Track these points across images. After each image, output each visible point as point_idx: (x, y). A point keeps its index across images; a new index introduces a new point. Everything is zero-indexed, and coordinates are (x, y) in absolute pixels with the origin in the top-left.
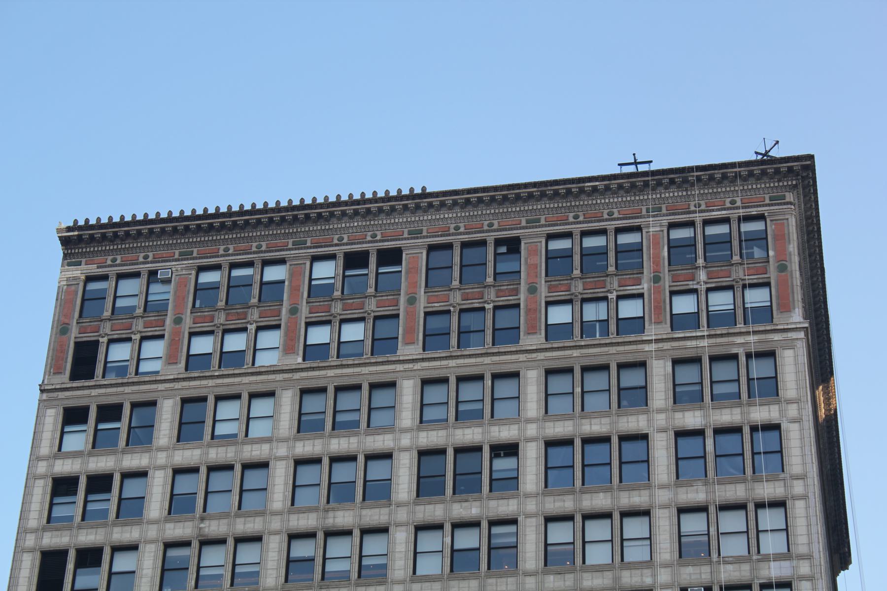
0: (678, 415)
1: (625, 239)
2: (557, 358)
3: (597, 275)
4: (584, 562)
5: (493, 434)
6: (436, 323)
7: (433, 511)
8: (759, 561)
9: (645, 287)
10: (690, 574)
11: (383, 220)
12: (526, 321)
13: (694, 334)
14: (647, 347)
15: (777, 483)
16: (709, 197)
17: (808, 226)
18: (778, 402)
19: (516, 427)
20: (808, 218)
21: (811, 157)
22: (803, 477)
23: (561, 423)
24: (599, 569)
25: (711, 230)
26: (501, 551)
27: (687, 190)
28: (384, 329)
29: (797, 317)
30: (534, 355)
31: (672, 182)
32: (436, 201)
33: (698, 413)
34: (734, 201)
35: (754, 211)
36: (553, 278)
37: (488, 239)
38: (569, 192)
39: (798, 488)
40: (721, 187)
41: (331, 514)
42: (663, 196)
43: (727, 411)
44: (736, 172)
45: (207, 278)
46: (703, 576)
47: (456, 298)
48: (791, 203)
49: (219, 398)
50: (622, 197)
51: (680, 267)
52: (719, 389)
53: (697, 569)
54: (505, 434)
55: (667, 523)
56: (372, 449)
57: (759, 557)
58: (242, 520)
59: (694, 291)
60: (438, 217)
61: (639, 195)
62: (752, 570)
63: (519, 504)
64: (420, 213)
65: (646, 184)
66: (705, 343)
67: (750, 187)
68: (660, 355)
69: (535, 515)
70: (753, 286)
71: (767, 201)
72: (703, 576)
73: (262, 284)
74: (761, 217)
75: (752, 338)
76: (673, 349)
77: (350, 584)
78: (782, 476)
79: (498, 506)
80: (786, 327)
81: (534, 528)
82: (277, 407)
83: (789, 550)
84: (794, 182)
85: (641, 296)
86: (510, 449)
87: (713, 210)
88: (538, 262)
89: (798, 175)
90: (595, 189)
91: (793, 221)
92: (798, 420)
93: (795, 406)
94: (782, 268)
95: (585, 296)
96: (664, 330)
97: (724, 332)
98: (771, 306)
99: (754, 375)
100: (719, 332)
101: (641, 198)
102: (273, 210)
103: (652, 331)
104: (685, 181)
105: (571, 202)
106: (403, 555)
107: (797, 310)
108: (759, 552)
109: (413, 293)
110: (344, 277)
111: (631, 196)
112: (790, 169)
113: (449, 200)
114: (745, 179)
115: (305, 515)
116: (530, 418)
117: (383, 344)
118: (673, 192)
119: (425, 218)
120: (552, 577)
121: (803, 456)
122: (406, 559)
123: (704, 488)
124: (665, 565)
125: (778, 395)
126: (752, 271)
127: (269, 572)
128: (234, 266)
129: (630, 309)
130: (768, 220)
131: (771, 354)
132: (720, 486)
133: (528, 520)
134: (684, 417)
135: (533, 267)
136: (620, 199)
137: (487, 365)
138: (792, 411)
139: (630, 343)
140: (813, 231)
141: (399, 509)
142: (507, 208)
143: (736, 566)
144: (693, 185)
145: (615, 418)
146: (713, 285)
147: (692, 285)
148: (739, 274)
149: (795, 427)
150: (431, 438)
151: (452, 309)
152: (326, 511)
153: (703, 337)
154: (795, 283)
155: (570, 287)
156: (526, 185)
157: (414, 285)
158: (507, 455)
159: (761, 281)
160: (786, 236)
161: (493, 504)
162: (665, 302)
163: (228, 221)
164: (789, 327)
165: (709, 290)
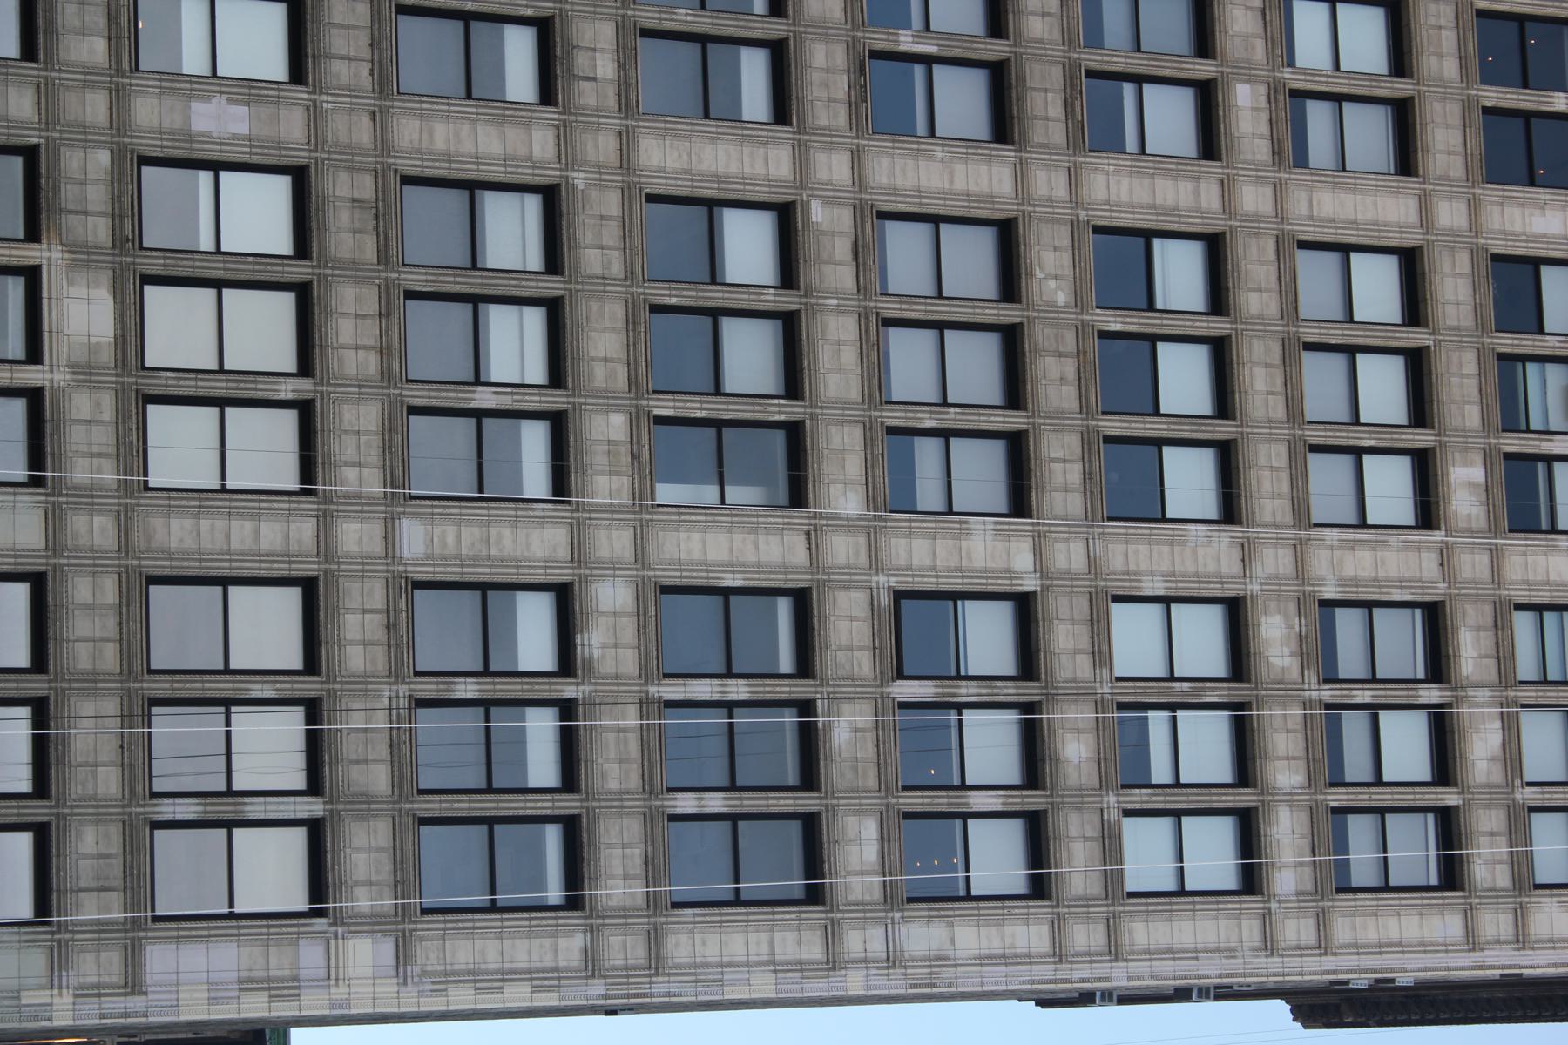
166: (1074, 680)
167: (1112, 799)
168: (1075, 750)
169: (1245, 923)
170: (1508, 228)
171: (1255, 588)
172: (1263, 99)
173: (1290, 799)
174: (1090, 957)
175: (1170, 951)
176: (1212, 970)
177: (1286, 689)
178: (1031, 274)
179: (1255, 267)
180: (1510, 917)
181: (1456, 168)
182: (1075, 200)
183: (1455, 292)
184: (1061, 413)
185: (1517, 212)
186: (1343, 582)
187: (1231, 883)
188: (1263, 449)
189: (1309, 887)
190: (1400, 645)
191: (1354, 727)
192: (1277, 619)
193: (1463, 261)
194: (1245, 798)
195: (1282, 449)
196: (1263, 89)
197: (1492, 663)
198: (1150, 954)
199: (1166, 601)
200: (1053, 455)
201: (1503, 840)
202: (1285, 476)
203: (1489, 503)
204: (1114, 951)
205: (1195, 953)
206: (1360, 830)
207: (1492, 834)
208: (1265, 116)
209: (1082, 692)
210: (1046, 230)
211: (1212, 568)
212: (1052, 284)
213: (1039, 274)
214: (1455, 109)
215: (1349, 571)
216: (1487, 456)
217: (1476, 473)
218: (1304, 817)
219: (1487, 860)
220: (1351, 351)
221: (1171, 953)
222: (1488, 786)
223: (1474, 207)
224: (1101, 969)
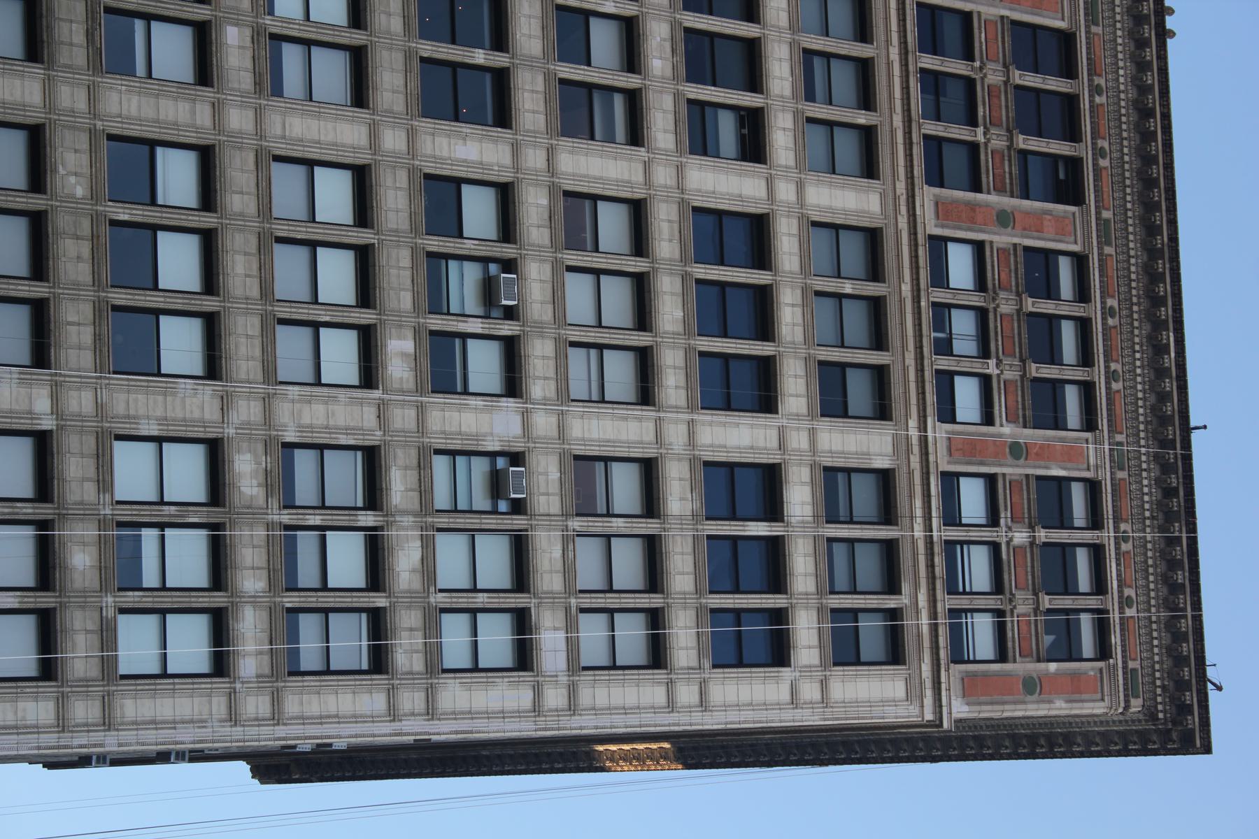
1: (1072, 397)
2: (898, 254)
3: (1025, 341)
4: (571, 269)
5: (780, 115)
6: (951, 31)
8: (567, 610)
9: (1006, 430)
10: (546, 474)
12: (955, 202)
13: (934, 514)
14: (913, 423)
15: (694, 653)
16: (1137, 559)
17: (1085, 735)
18: (823, 665)
19: (792, 163)
20: (910, 740)
21: (1207, 749)
23: (796, 249)
24: (558, 297)
25: (1082, 560)
27: (1153, 518)
29: (959, 709)
30: (903, 209)
31: (1169, 493)
32: (1151, 54)
33: (808, 510)
34: (1131, 603)
35: (1116, 639)
36: (1021, 259)
37: (1083, 145)
39: (687, 694)
40: (1156, 582)
42: (1144, 474)
43: (811, 569)
44: (1184, 610)
46: (543, 499)
47: (994, 76)
48: (1127, 707)
50: (1144, 399)
51: (1033, 496)
52: (839, 550)
53: (554, 488)
54: (781, 138)
55: (633, 437)
57: (574, 610)
60: (1120, 56)
61: (1146, 430)
62: (552, 595)
63: (666, 152)
64: (1129, 23)
65: (1166, 444)
66: (919, 533)
67: (1155, 634)
68: (901, 447)
69: (648, 181)
70: (1000, 631)
71: (1131, 665)
74: (1104, 651)
75: (925, 621)
76: (910, 473)
78: (707, 664)
79: (664, 112)
80: (943, 686)
81: (626, 177)
83: (585, 669)
84: (1161, 715)
86: (753, 148)
87: (1118, 565)
88: (1045, 235)
89: (1174, 723)
90: (1160, 350)
91: (1097, 708)
92: (794, 701)
93: (817, 696)
94: (1031, 686)
95: (991, 316)
96: (942, 462)
97: (938, 571)
98: (969, 662)
100: (937, 560)
101: (1142, 435)
103: (938, 432)
105: (1139, 304)
107: (966, 708)
108: (583, 611)
111: (1145, 415)
112: (1188, 709)
113: (1152, 78)
116: (799, 192)
118: (1150, 494)
119: (1119, 33)
120: (545, 202)
121: (738, 706)
123: (689, 513)
124: (561, 428)
125: (835, 664)
126: (1024, 627)
129: (967, 394)
130: (1101, 664)
131: (895, 654)
132: (690, 540)
133: (640, 167)
134: (803, 483)
135: (1035, 224)
136: (1140, 395)
137: (889, 119)
138: (810, 691)
140: (916, 748)
142: (1132, 186)
143: (559, 565)
144: (1162, 529)
145: (803, 352)
146: (1004, 556)
147: (1005, 517)
148: (1023, 604)
149: (785, 696)
151: (977, 64)
153: (928, 528)
154: (1007, 707)
155: (1006, 290)
156: (1173, 223)
158: (742, 140)
159: (1010, 644)
160: (1076, 696)
161: (668, 102)
162: (982, 464)
164: (944, 693)
165: (995, 547)
166: (81, 503)
167: (110, 599)
168: (80, 560)
169: (215, 700)
170: (438, 153)
171: (231, 431)
172: (249, 39)
173: (254, 600)
174: (87, 727)
175: (154, 722)
176: (187, 738)
177: (253, 513)
178: (55, 171)
179: (238, 174)
180: (423, 695)
181: (399, 105)
182: (93, 113)
183: (396, 201)
184: (77, 285)
185: (445, 141)
186: (301, 428)
187: (204, 666)
188: (241, 320)
189: (267, 671)
190: (344, 479)
191: (306, 543)
192: (248, 456)
193: (402, 178)
194: (218, 600)
195: (256, 321)
196: (248, 32)
197: (416, 495)
198: (137, 724)
199: (159, 440)
200: (70, 319)
201: (420, 634)
202: (257, 342)
203: (417, 369)
204: (108, 722)
205: (174, 724)
206: (309, 625)
207: (411, 629)
208: (249, 54)
209: (87, 513)
210: (68, 134)
211: (197, 415)
212: (73, 179)
213: (61, 170)
214: (398, 58)
215: (306, 420)
216: (417, 332)
217: (408, 345)
218: (265, 615)
219: (406, 650)
220: (313, 245)
221: (155, 723)
222: (409, 591)
223: (412, 135)
224: (96, 737)
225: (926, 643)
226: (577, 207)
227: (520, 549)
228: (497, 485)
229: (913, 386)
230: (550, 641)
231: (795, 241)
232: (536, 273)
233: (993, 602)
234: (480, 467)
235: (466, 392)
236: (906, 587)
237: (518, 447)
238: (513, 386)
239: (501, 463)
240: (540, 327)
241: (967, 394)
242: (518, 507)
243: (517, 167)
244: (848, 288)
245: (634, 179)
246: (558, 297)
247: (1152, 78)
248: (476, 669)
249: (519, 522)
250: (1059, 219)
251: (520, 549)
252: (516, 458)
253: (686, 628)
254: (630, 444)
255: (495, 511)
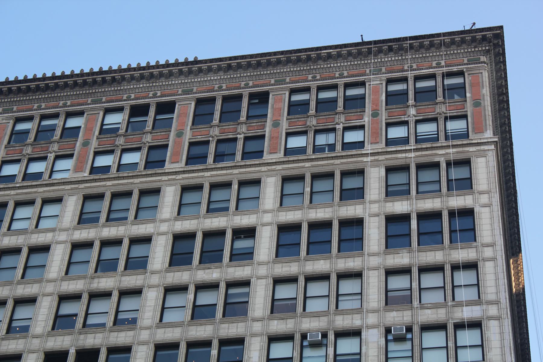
0: (389, 205)
1: (351, 92)
2: (293, 169)
3: (328, 113)
4: (304, 309)
5: (235, 221)
6: (198, 150)
7: (181, 276)
8: (453, 306)
9: (366, 119)
10: (394, 317)
11: (163, 82)
12: (269, 146)
13: (404, 148)
14: (365, 159)
15: (470, 250)
17: (497, 80)
18: (473, 193)
19: (255, 216)
20: (504, 155)
21: (501, 27)
22: (492, 245)
24: (317, 315)
25: (421, 84)
26: (236, 305)
27: (402, 56)
28: (156, 156)
29: (489, 134)
30: (273, 167)
31: (390, 49)
32: (204, 66)
33: (405, 203)
34: (439, 63)
35: (455, 69)
36: (293, 117)
37: (244, 93)
38: (309, 58)
39: (488, 252)
40: (429, 53)
41: (96, 280)
42: (383, 60)
43: (430, 200)
44: (441, 40)
45: (21, 127)
46: (405, 319)
47: (216, 132)
48: (484, 63)
49: (18, 204)
50: (351, 61)
51: (394, 106)
52: (422, 188)
53: (400, 314)
54: (244, 221)
55: (376, 280)
56: (135, 234)
57: (453, 303)
58: (23, 286)
59: (406, 123)
60: (206, 79)
61: (364, 60)
62: (447, 313)
63: (253, 270)
64: (192, 76)
65: (369, 52)
66: (412, 155)
67: (452, 52)
69: (265, 277)
70: (453, 118)
71: (466, 62)
72: (405, 319)
73: (64, 129)
74: (461, 74)
75: (451, 151)
76: (387, 159)
77: (105, 330)
78: (474, 244)
80: (479, 141)
81: (264, 287)
82: (63, 211)
83: (479, 297)
84: (487, 48)
85: (362, 127)
86: (249, 233)
87: (423, 69)
88: (282, 106)
89: (490, 42)
90: (329, 56)
91: (486, 74)
92: (489, 205)
93: (486, 196)
94: (477, 104)
95: (318, 128)
96: (381, 146)
97: (429, 146)
98: (468, 131)
99: (453, 176)
100: (424, 146)
101: (366, 62)
102: (77, 75)
103: (369, 148)
104: (401, 48)
105: (310, 66)
106: (152, 308)
107: (488, 131)
108: (454, 299)
109: (182, 129)
110: (129, 122)
111: (358, 61)
113: (215, 65)
114: (448, 46)
115: (75, 281)
116: (267, 212)
117: (154, 162)
118: (391, 57)
119: (196, 80)
120: (276, 322)
121: (492, 230)
122: (154, 311)
124: (374, 311)
125: (472, 188)
126: (452, 108)
127: (39, 323)
128: (44, 117)
129: (352, 137)
130: (466, 74)
131: (466, 163)
132: (420, 253)
133: (259, 281)
134: (393, 205)
135: (278, 111)
136: (349, 63)
137: (234, 175)
138: (484, 199)
139: (352, 156)
140: (507, 152)
141: (153, 275)
142: (260, 71)
144: (406, 51)
145: (336, 208)
146: (421, 118)
148: (442, 109)
149: (487, 209)
150: (184, 226)
151: (211, 139)
152: (93, 278)
154: (487, 114)
155: (306, 123)
156: (275, 53)
157: (184, 124)
159: (459, 114)
160: (481, 84)
161: (231, 270)
162: (381, 129)
163: (42, 84)
164: (482, 141)
165: (417, 122)
225: (461, 149)
226: (276, 307)
227: (426, 328)
228: (400, 339)
229: (349, 160)
230: (468, 313)
231: (289, 213)
232: (307, 324)
233: (441, 122)
234: (392, 346)
235: (360, 354)
236: (437, 159)
237: (383, 330)
238: (356, 333)
239: (390, 337)
240: (329, 322)
241: (352, 137)
242: (409, 329)
243: (261, 335)
244: (308, 189)
245: (264, 284)
246: (317, 315)
247: (215, 65)
248: (482, 346)
249: (416, 329)
250: (275, 101)
251: (426, 328)
252: (388, 331)
253: (459, 254)
254: (379, 281)
255: (412, 339)
